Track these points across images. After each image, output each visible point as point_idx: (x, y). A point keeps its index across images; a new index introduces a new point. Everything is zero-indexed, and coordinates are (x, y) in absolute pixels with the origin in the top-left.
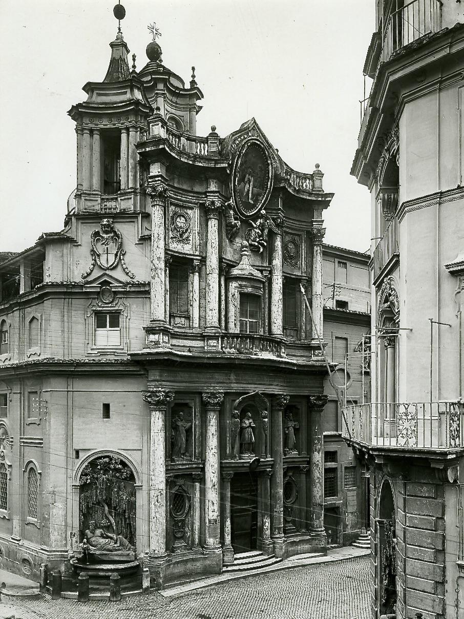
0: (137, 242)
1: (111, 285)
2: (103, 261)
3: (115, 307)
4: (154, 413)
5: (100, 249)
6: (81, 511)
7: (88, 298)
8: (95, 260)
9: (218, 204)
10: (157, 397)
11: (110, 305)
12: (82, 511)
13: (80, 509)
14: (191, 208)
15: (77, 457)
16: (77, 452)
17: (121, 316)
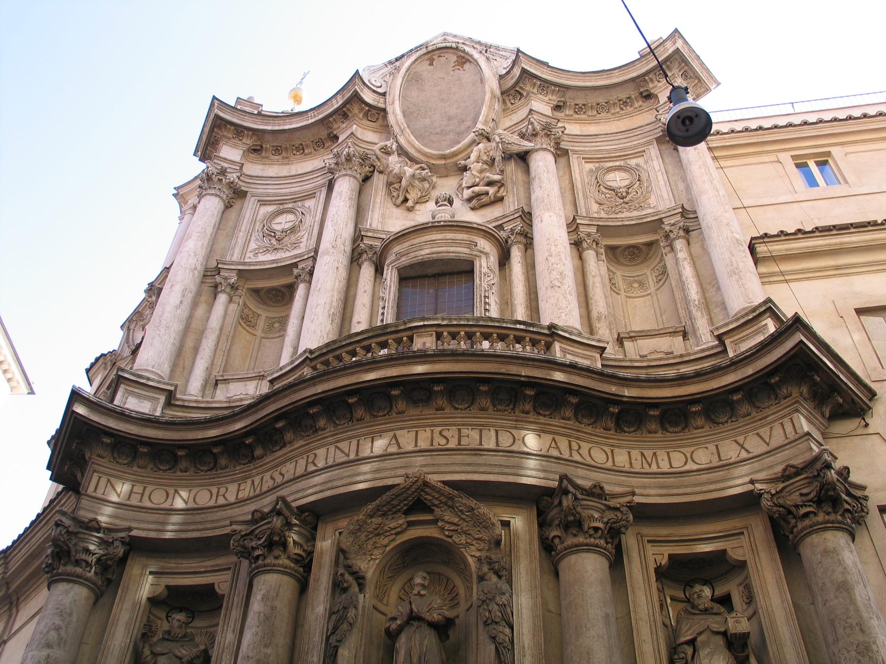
14: (311, 196)
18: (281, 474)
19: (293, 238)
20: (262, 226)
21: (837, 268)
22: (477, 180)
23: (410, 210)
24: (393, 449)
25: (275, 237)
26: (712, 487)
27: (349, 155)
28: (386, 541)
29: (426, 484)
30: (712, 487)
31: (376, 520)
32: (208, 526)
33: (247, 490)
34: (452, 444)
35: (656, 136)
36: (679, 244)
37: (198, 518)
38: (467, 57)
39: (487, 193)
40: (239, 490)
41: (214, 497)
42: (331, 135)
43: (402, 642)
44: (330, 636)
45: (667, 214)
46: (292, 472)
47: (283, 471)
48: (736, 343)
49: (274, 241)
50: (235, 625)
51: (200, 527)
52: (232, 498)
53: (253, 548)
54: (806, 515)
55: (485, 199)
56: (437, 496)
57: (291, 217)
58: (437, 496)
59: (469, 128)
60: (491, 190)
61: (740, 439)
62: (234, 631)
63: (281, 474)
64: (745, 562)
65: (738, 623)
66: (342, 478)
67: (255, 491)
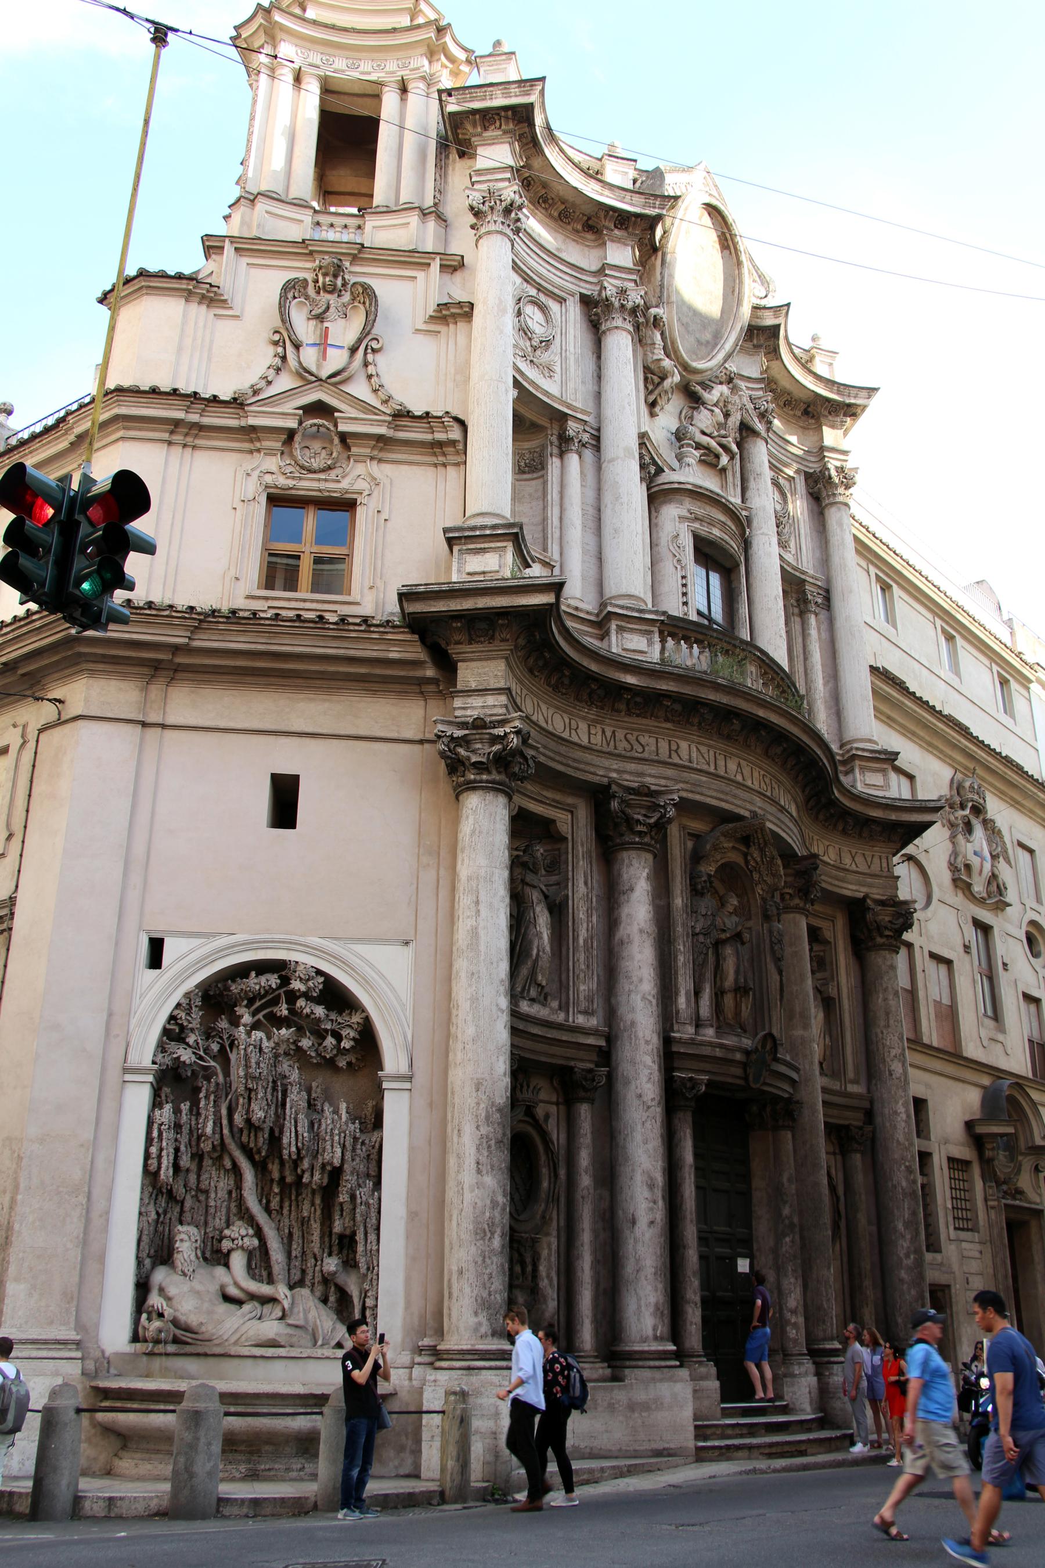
0: (424, 327)
1: (336, 414)
2: (309, 357)
3: (339, 481)
4: (473, 801)
5: (304, 328)
6: (150, 1175)
7: (251, 452)
8: (284, 358)
9: (635, 297)
10: (495, 739)
11: (322, 476)
12: (156, 1174)
13: (146, 1165)
15: (155, 959)
16: (156, 947)
17: (359, 509)
18: (637, 740)
19: (544, 357)
20: (517, 307)
21: (889, 717)
22: (716, 434)
23: (652, 415)
24: (739, 778)
25: (530, 339)
26: (836, 883)
27: (638, 306)
28: (718, 858)
29: (763, 828)
30: (836, 883)
31: (722, 839)
32: (571, 763)
33: (599, 737)
34: (769, 794)
35: (807, 470)
36: (812, 620)
37: (563, 749)
38: (730, 243)
39: (717, 457)
40: (590, 734)
41: (568, 729)
42: (590, 222)
43: (728, 951)
44: (697, 934)
45: (811, 580)
46: (654, 748)
47: (642, 740)
48: (862, 769)
49: (528, 344)
50: (585, 877)
51: (565, 761)
52: (585, 741)
53: (638, 821)
54: (887, 936)
55: (711, 459)
56: (760, 836)
57: (538, 316)
58: (760, 836)
59: (708, 342)
60: (724, 460)
61: (854, 851)
62: (586, 883)
63: (637, 740)
64: (829, 943)
65: (833, 992)
66: (710, 789)
67: (608, 745)
